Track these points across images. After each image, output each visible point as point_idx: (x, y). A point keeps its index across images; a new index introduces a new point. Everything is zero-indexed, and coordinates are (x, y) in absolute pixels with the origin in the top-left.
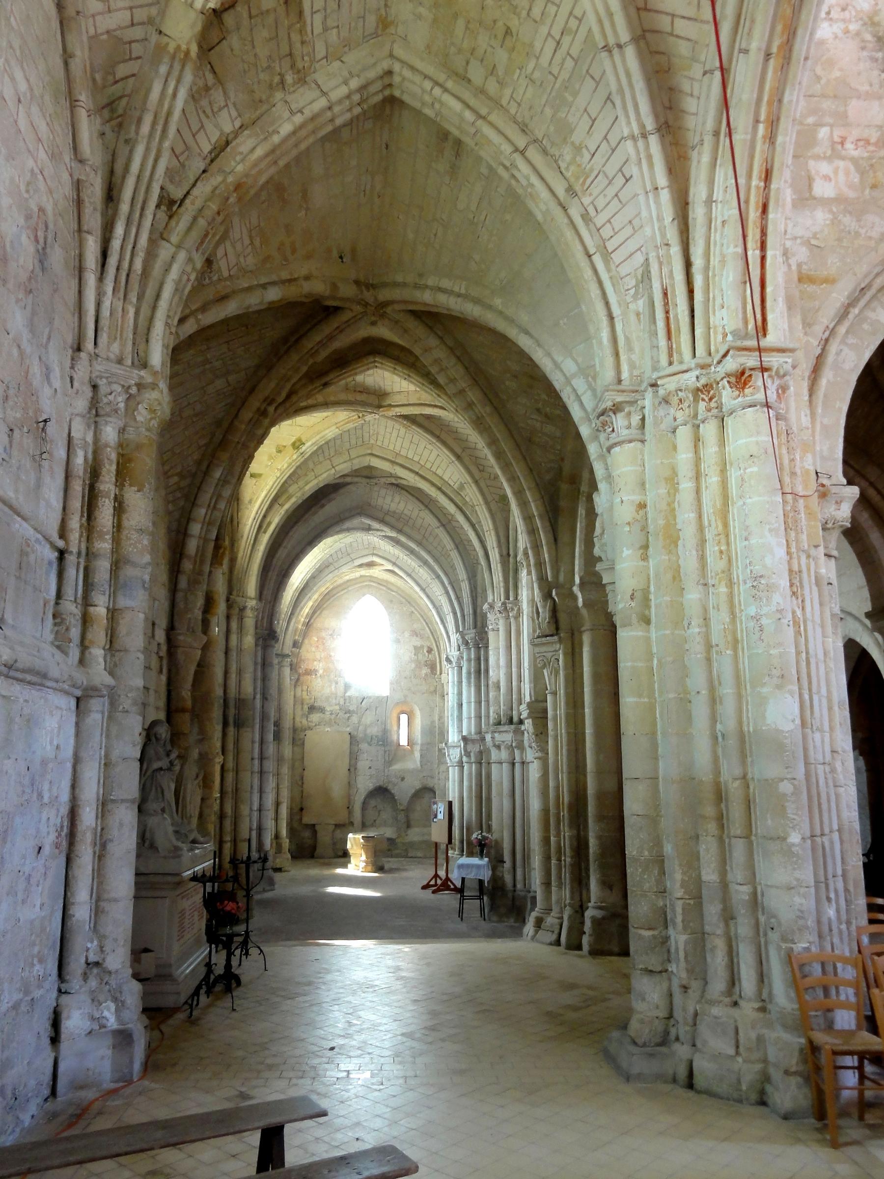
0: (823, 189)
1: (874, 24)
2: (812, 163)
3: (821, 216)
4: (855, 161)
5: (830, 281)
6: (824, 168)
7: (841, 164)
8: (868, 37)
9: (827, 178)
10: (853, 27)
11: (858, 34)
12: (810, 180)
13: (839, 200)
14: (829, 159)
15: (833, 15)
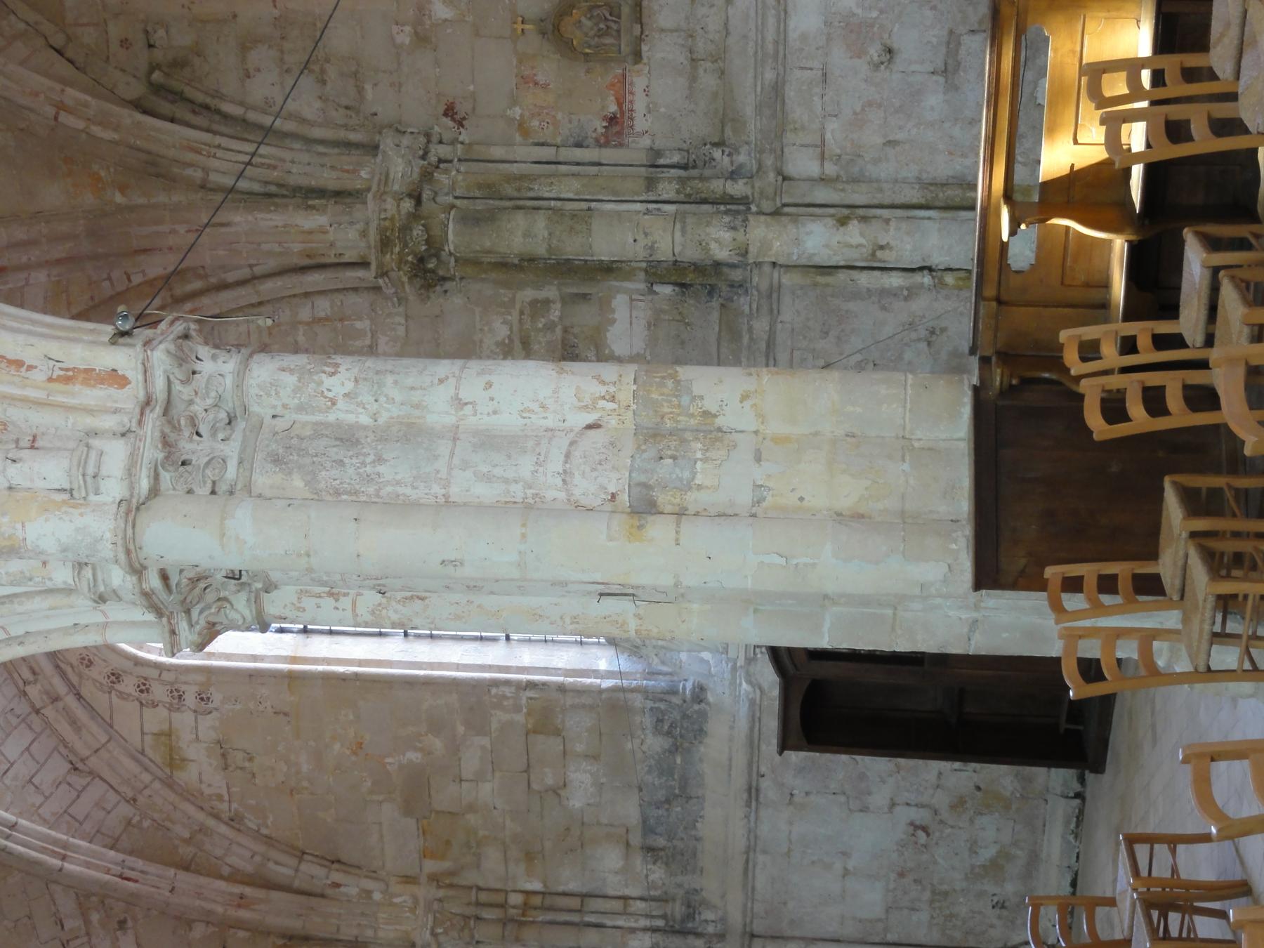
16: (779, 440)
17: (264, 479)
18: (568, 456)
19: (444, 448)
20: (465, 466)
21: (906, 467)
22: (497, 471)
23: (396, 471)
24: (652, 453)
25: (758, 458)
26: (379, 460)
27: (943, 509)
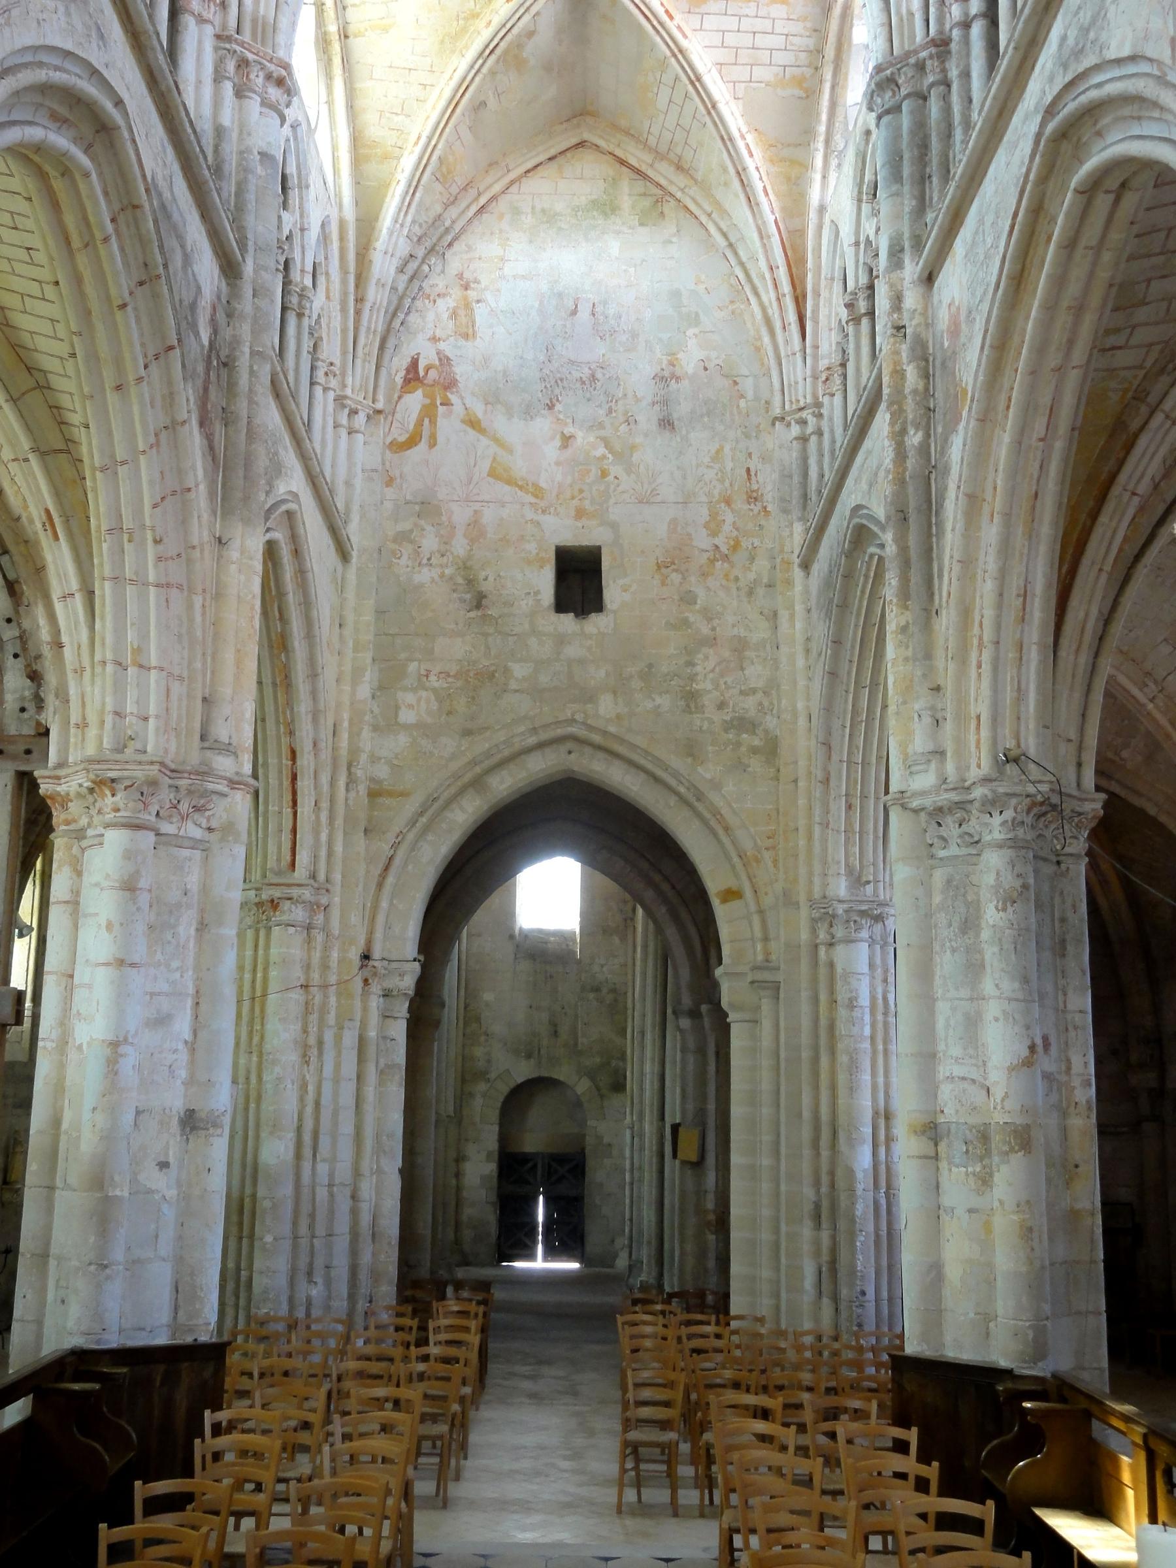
0: (407, 716)
1: (466, 568)
2: (400, 694)
3: (403, 739)
4: (434, 690)
5: (404, 794)
6: (410, 698)
7: (424, 694)
8: (460, 580)
9: (410, 706)
10: (447, 572)
11: (451, 578)
12: (397, 708)
13: (420, 726)
14: (414, 690)
15: (433, 561)
16: (988, 1227)
17: (939, 876)
18: (964, 1079)
19: (964, 993)
20: (954, 1009)
21: (972, 1315)
22: (951, 1032)
23: (946, 963)
24: (969, 1136)
25: (970, 1211)
26: (954, 950)
27: (948, 1338)
